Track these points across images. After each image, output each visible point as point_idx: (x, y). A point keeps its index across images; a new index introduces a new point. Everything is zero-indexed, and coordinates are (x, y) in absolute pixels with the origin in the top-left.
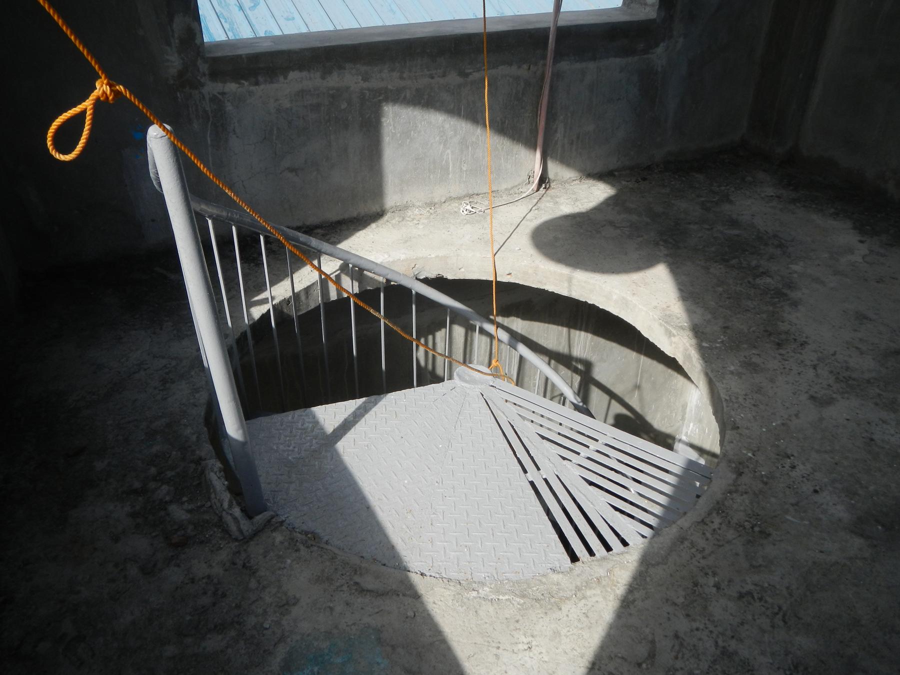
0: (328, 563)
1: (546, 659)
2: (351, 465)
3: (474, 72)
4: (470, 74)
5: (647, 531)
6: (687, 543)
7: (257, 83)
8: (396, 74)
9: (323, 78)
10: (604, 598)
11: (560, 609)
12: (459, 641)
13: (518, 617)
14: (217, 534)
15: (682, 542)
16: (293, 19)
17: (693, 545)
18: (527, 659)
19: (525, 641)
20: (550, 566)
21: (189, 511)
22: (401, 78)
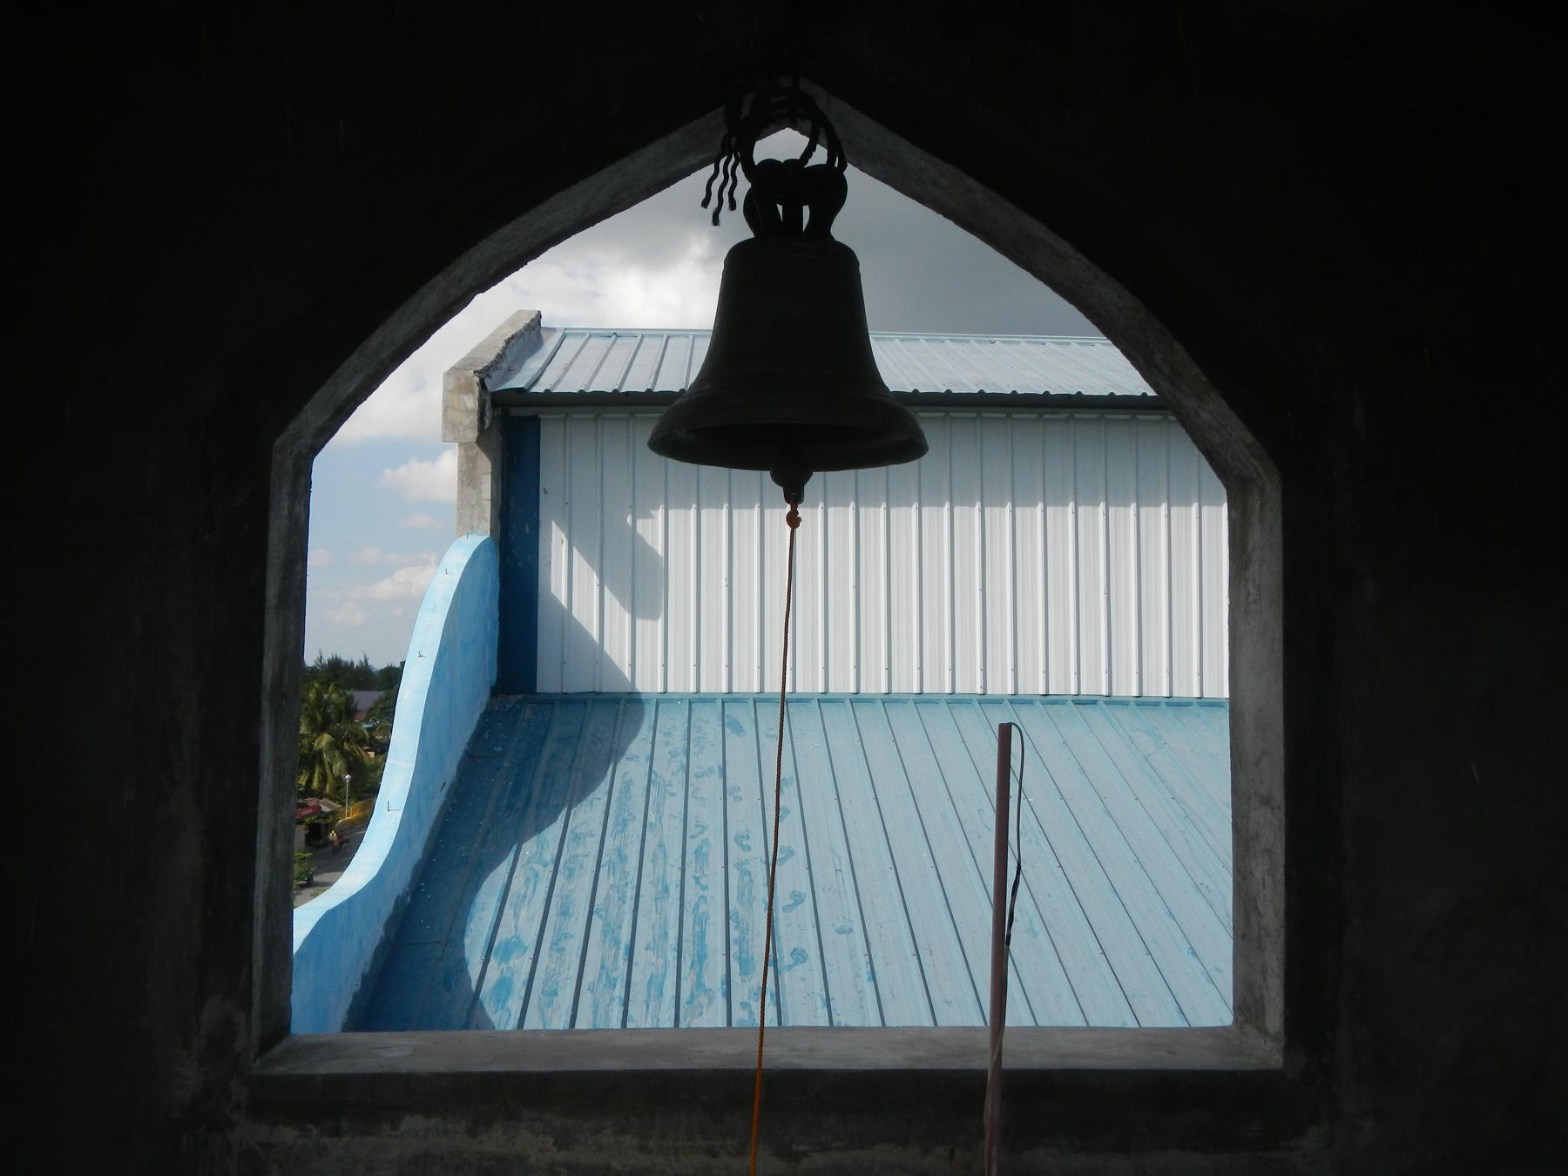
3: (813, 1151)
4: (805, 1154)
7: (336, 1133)
8: (629, 1140)
9: (472, 1133)
16: (851, 930)
22: (642, 1149)
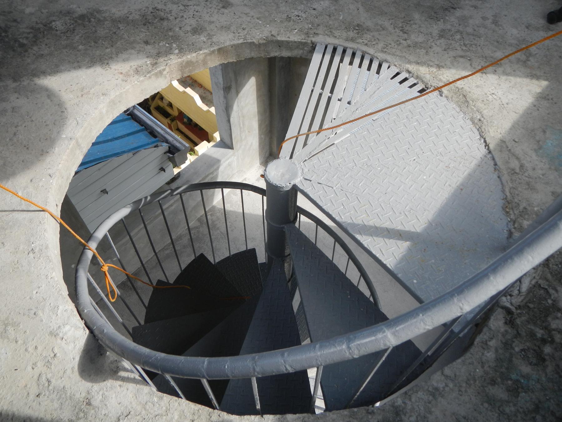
0: (520, 189)
1: (494, 88)
2: (434, 214)
5: (385, 66)
6: (385, 50)
10: (443, 74)
11: (463, 88)
12: (512, 119)
13: (480, 101)
14: (552, 262)
15: (386, 52)
17: (384, 48)
18: (500, 93)
19: (490, 97)
20: (439, 96)
21: (557, 291)
